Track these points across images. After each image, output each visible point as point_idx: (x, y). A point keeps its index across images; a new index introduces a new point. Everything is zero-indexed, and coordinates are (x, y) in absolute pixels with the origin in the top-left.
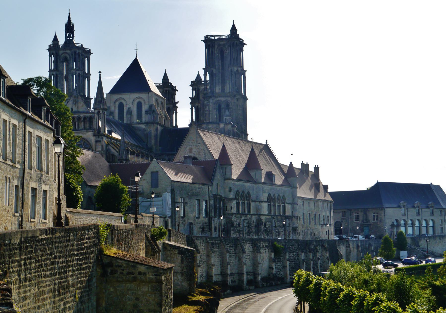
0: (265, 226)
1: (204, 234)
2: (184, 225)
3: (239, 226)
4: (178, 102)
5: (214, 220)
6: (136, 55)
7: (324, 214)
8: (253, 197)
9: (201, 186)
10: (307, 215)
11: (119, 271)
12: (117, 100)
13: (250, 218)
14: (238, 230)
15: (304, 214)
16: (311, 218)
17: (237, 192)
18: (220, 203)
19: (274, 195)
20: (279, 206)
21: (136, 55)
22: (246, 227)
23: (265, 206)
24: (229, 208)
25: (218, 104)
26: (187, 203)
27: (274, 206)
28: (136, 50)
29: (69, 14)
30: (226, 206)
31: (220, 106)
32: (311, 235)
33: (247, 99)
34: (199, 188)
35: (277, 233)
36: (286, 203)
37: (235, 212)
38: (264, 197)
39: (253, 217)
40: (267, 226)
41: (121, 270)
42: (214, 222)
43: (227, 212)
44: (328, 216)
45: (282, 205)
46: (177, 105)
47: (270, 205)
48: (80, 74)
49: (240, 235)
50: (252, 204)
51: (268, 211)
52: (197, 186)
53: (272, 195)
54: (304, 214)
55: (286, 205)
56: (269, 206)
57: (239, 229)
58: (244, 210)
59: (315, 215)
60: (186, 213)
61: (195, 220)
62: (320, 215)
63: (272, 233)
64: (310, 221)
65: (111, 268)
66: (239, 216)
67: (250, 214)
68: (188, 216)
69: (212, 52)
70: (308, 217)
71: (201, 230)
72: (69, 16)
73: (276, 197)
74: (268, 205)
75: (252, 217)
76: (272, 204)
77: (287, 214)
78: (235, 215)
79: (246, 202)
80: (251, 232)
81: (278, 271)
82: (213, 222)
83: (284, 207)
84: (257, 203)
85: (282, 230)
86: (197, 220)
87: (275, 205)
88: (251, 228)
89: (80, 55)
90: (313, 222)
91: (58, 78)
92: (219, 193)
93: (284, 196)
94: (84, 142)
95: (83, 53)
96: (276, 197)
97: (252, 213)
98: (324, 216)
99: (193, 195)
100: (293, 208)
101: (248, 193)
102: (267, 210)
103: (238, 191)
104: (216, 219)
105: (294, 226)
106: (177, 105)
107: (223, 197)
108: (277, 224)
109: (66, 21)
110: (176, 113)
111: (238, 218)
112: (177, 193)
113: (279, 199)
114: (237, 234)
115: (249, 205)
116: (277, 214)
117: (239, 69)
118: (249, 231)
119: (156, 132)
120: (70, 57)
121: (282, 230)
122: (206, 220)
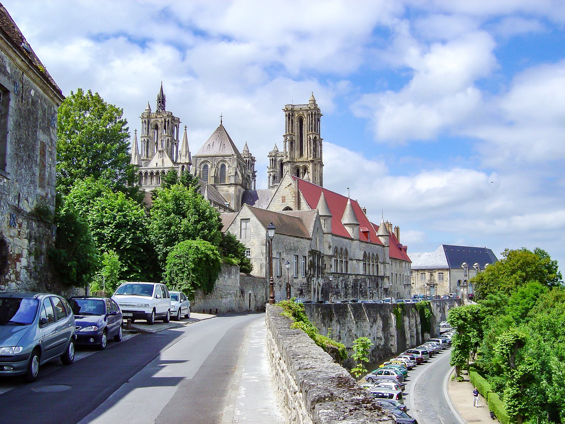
0: (361, 288)
1: (302, 297)
2: (280, 286)
3: (337, 287)
5: (313, 281)
6: (221, 121)
7: (406, 274)
8: (351, 254)
10: (394, 275)
12: (202, 163)
14: (336, 292)
15: (392, 273)
16: (397, 278)
18: (318, 261)
19: (369, 254)
21: (221, 121)
22: (344, 288)
24: (328, 266)
25: (296, 169)
27: (369, 264)
28: (221, 117)
29: (162, 86)
30: (325, 264)
31: (298, 171)
32: (397, 296)
36: (379, 262)
37: (333, 272)
39: (350, 277)
42: (313, 283)
43: (326, 271)
47: (365, 264)
48: (169, 139)
49: (337, 297)
50: (350, 262)
51: (363, 270)
52: (296, 239)
54: (392, 273)
55: (379, 264)
57: (337, 290)
61: (293, 281)
63: (366, 295)
69: (292, 120)
72: (162, 88)
76: (367, 263)
80: (348, 294)
83: (378, 265)
84: (354, 262)
85: (375, 291)
86: (295, 281)
89: (170, 122)
91: (149, 143)
92: (318, 249)
95: (173, 121)
97: (349, 273)
99: (291, 249)
101: (346, 250)
103: (336, 248)
105: (386, 287)
107: (322, 254)
109: (158, 92)
110: (255, 181)
113: (373, 258)
114: (335, 296)
117: (317, 136)
118: (346, 292)
119: (238, 193)
121: (375, 291)
122: (305, 280)
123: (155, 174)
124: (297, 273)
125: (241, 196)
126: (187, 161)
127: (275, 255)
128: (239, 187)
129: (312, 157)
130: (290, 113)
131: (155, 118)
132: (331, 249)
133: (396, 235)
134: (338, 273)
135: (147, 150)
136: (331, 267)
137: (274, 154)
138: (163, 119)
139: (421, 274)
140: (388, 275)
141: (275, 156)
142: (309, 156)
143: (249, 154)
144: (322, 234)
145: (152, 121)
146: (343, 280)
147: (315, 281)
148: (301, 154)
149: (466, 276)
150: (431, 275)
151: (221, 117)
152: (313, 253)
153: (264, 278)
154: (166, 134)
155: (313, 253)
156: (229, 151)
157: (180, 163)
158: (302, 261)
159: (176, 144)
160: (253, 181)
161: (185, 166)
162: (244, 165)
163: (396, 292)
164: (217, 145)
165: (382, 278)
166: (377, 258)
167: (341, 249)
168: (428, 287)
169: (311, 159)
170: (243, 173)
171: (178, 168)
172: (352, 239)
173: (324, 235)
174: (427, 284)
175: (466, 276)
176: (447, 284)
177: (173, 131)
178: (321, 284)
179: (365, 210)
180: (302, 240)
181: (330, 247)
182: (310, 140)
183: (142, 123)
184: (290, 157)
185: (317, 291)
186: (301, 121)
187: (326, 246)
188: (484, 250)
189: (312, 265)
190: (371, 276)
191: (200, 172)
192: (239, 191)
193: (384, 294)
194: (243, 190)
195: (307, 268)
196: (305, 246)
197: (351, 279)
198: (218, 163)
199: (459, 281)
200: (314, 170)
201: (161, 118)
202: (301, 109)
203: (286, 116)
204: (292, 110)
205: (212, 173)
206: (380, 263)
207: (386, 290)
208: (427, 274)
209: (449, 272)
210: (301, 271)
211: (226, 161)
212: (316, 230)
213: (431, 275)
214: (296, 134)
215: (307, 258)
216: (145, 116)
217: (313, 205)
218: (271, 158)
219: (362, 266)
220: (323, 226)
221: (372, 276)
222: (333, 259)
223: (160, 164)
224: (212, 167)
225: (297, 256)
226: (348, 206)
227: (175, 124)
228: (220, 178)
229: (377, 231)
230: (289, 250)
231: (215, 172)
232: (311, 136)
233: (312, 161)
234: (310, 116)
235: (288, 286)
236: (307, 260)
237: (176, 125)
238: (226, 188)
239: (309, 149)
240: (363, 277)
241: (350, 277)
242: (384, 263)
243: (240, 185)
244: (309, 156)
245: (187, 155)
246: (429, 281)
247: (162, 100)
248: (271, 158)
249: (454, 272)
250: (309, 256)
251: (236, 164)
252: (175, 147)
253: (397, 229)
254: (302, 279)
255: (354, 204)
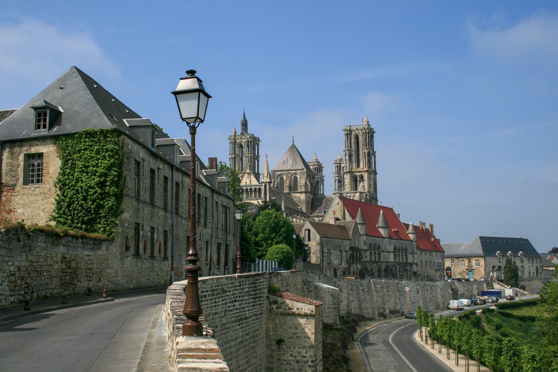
2: (330, 270)
4: (325, 176)
5: (352, 266)
6: (293, 141)
7: (437, 261)
8: (383, 248)
9: (342, 240)
10: (424, 263)
11: (283, 307)
13: (380, 265)
14: (371, 274)
15: (421, 261)
17: (370, 245)
18: (357, 253)
19: (399, 247)
20: (402, 255)
21: (293, 141)
22: (377, 271)
23: (392, 255)
24: (364, 257)
26: (331, 253)
28: (293, 137)
30: (362, 256)
31: (356, 179)
32: (427, 277)
33: (377, 173)
34: (341, 242)
35: (401, 276)
37: (369, 260)
38: (391, 248)
39: (383, 263)
40: (393, 271)
41: (284, 306)
43: (362, 260)
44: (441, 263)
45: (404, 254)
46: (324, 178)
50: (382, 254)
51: (394, 259)
52: (340, 240)
53: (397, 247)
54: (421, 261)
55: (408, 254)
56: (395, 255)
57: (372, 272)
58: (375, 258)
59: (430, 262)
60: (331, 260)
62: (434, 262)
63: (397, 276)
64: (426, 267)
65: (277, 305)
66: (372, 263)
67: (380, 262)
68: (333, 263)
69: (350, 138)
70: (425, 264)
71: (343, 273)
72: (244, 114)
73: (400, 248)
74: (394, 254)
75: (381, 264)
76: (397, 253)
77: (409, 261)
78: (368, 262)
79: (377, 252)
81: (402, 306)
82: (352, 267)
83: (407, 255)
84: (386, 253)
85: (405, 274)
86: (340, 266)
87: (399, 255)
88: (381, 272)
90: (428, 268)
93: (406, 247)
94: (255, 207)
95: (254, 141)
96: (400, 248)
97: (381, 261)
98: (437, 263)
100: (413, 257)
101: (379, 246)
102: (393, 258)
103: (371, 244)
104: (354, 265)
105: (414, 271)
106: (324, 178)
108: (401, 269)
109: (242, 118)
110: (323, 184)
111: (371, 264)
112: (325, 245)
113: (402, 250)
114: (370, 276)
115: (379, 254)
116: (401, 262)
117: (371, 151)
118: (379, 274)
119: (308, 199)
120: (245, 144)
121: (405, 274)
122: (346, 266)
123: (245, 191)
124: (341, 261)
125: (310, 201)
126: (268, 180)
127: (326, 250)
128: (309, 194)
129: (367, 168)
130: (349, 133)
131: (240, 139)
132: (366, 245)
133: (430, 230)
134: (373, 261)
135: (235, 165)
136: (367, 257)
137: (338, 162)
138: (246, 139)
139: (476, 260)
140: (416, 262)
141: (340, 163)
142: (364, 167)
143: (317, 162)
144: (359, 236)
145: (238, 141)
146: (376, 266)
147: (354, 266)
148: (358, 166)
149: (500, 262)
150: (470, 261)
151: (293, 137)
152: (352, 248)
153: (319, 265)
154: (250, 152)
155: (352, 248)
156: (300, 165)
157: (263, 182)
158: (344, 254)
159: (257, 159)
160: (322, 185)
161: (267, 184)
162: (313, 176)
163: (426, 275)
164: (290, 161)
165: (411, 264)
166: (406, 249)
167: (375, 245)
168: (467, 271)
169: (366, 169)
170: (312, 182)
171: (262, 185)
172: (384, 238)
173: (361, 237)
174: (467, 270)
175: (500, 262)
176: (482, 269)
177: (254, 149)
178: (359, 268)
179: (399, 215)
180: (344, 241)
181: (365, 244)
182: (365, 154)
183: (230, 143)
184: (349, 168)
185: (356, 273)
186: (357, 137)
187: (362, 243)
188: (521, 239)
189: (352, 256)
190: (401, 263)
191: (277, 182)
192: (309, 197)
193: (413, 276)
194: (311, 196)
195: (348, 258)
196: (347, 244)
197: (383, 265)
198: (292, 175)
199: (494, 267)
200: (369, 178)
201: (245, 139)
202: (357, 129)
203: (345, 135)
204: (350, 131)
205: (287, 183)
206: (409, 253)
207: (415, 273)
208: (466, 261)
209: (483, 260)
210: (344, 260)
211: (297, 174)
212: (354, 233)
213: (470, 261)
214: (354, 149)
215: (348, 252)
216: (232, 138)
217: (353, 216)
218: (336, 165)
219: (393, 256)
220: (360, 230)
221: (402, 263)
222: (368, 252)
223: (248, 183)
224: (286, 179)
225: (341, 251)
226: (381, 215)
227: (256, 142)
228: (294, 187)
229: (407, 229)
230: (336, 248)
231: (289, 183)
232: (366, 150)
233: (367, 171)
234: (365, 134)
235: (335, 270)
236: (348, 253)
237: (257, 144)
238: (298, 195)
239: (364, 161)
240: (393, 264)
241: (383, 263)
242: (413, 253)
243: (309, 193)
244: (364, 167)
245: (268, 176)
246: (468, 267)
247: (245, 124)
248: (336, 165)
249: (489, 259)
250: (349, 251)
251: (305, 176)
252: (256, 161)
253: (432, 226)
254: (344, 265)
255: (389, 211)
